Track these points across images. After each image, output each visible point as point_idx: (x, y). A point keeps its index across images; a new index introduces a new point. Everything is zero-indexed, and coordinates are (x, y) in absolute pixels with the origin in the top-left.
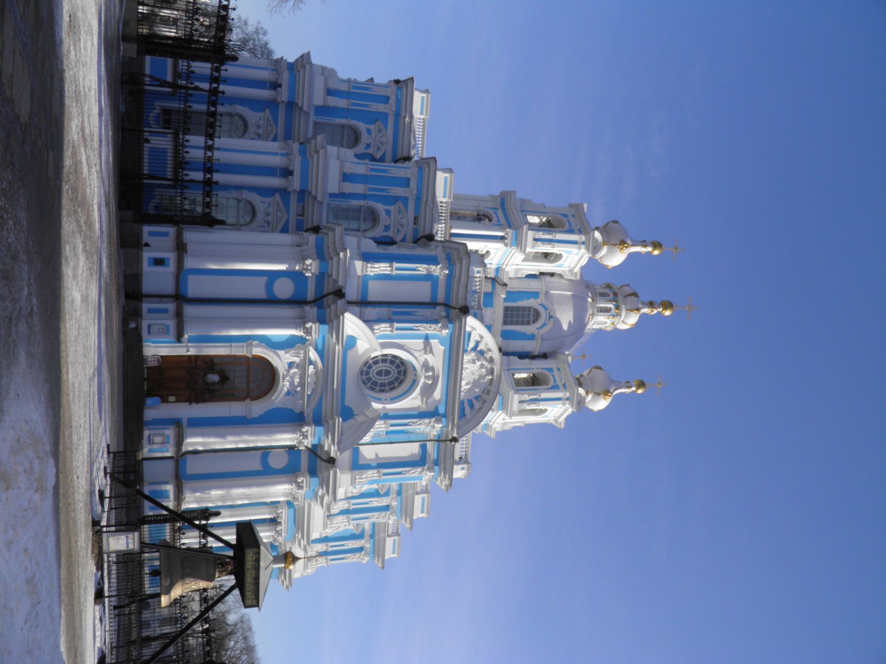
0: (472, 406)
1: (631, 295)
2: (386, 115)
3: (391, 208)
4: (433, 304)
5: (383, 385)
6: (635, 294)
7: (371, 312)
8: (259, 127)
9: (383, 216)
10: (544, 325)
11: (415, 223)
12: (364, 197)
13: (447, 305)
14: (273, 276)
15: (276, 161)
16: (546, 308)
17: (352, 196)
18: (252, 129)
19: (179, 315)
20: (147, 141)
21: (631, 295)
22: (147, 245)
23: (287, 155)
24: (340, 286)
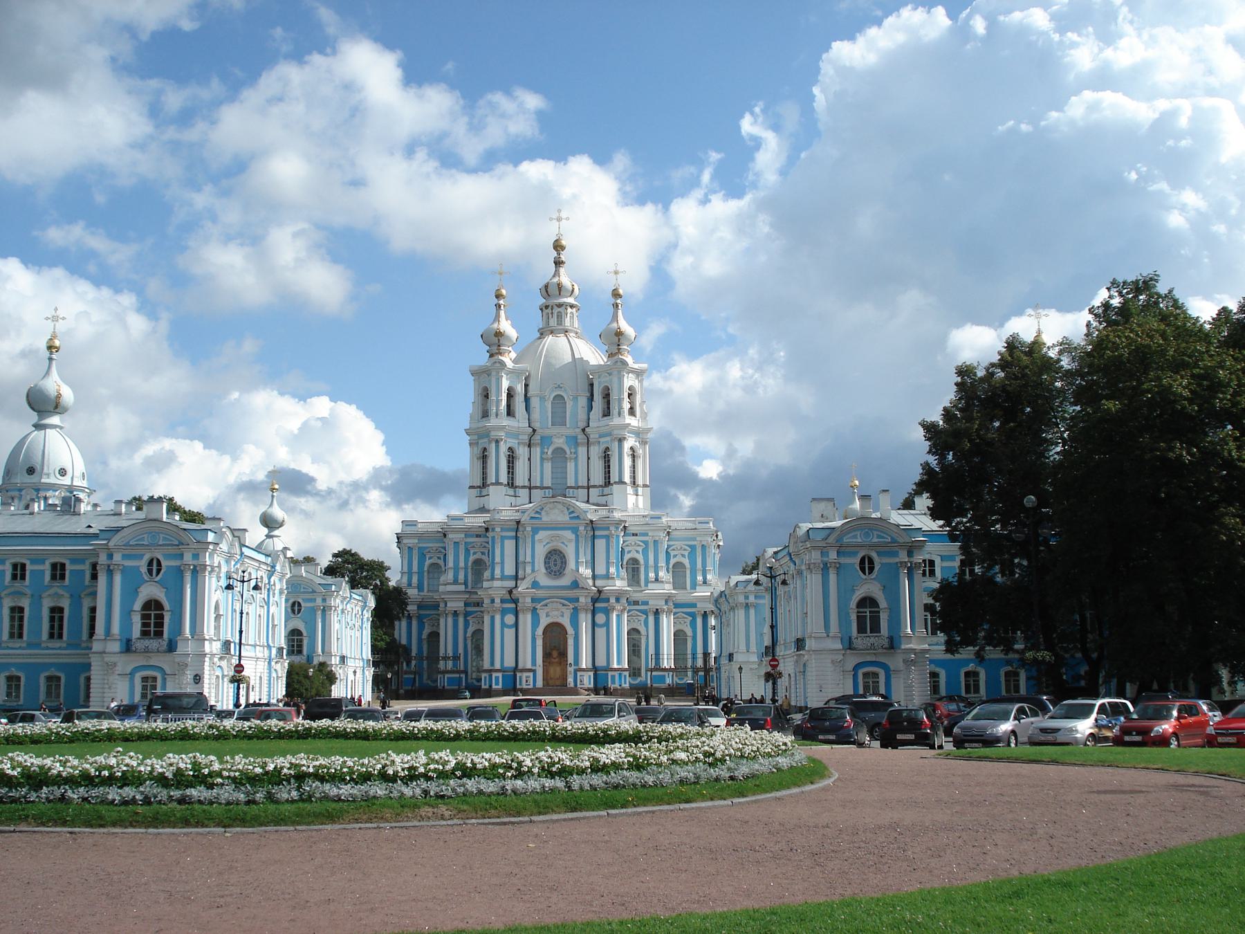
0: (573, 512)
1: (547, 291)
3: (472, 552)
4: (516, 538)
5: (562, 562)
6: (546, 287)
8: (433, 625)
9: (476, 557)
11: (480, 536)
12: (466, 568)
13: (517, 531)
14: (503, 625)
15: (450, 620)
17: (466, 576)
18: (435, 629)
19: (523, 670)
20: (444, 687)
21: (547, 291)
22: (491, 686)
23: (446, 614)
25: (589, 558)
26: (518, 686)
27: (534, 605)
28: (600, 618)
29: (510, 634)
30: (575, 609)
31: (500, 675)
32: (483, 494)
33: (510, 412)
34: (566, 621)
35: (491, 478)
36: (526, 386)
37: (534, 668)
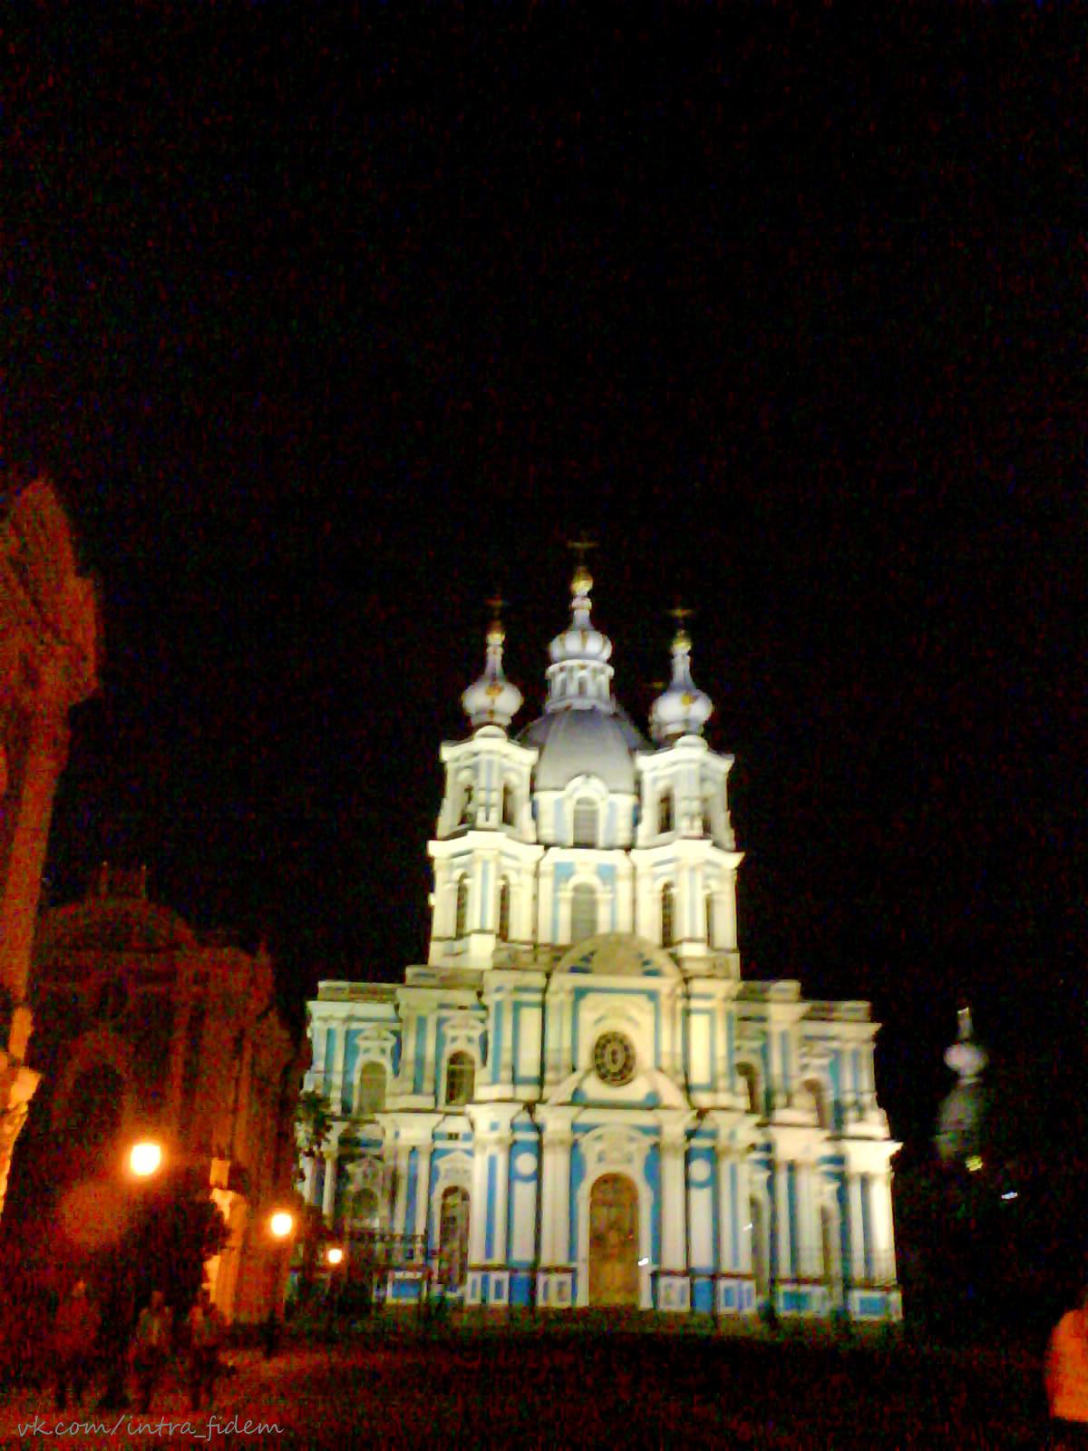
2: (348, 1033)
7: (549, 1076)
10: (597, 790)
13: (544, 991)
14: (512, 1177)
16: (576, 790)
19: (547, 1270)
24: (524, 1108)
25: (679, 1049)
26: (541, 1303)
27: (578, 1136)
28: (700, 1170)
29: (524, 1192)
30: (656, 1147)
31: (505, 1276)
32: (456, 951)
33: (507, 819)
34: (635, 1172)
35: (473, 921)
36: (533, 778)
37: (573, 1265)
